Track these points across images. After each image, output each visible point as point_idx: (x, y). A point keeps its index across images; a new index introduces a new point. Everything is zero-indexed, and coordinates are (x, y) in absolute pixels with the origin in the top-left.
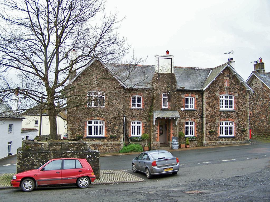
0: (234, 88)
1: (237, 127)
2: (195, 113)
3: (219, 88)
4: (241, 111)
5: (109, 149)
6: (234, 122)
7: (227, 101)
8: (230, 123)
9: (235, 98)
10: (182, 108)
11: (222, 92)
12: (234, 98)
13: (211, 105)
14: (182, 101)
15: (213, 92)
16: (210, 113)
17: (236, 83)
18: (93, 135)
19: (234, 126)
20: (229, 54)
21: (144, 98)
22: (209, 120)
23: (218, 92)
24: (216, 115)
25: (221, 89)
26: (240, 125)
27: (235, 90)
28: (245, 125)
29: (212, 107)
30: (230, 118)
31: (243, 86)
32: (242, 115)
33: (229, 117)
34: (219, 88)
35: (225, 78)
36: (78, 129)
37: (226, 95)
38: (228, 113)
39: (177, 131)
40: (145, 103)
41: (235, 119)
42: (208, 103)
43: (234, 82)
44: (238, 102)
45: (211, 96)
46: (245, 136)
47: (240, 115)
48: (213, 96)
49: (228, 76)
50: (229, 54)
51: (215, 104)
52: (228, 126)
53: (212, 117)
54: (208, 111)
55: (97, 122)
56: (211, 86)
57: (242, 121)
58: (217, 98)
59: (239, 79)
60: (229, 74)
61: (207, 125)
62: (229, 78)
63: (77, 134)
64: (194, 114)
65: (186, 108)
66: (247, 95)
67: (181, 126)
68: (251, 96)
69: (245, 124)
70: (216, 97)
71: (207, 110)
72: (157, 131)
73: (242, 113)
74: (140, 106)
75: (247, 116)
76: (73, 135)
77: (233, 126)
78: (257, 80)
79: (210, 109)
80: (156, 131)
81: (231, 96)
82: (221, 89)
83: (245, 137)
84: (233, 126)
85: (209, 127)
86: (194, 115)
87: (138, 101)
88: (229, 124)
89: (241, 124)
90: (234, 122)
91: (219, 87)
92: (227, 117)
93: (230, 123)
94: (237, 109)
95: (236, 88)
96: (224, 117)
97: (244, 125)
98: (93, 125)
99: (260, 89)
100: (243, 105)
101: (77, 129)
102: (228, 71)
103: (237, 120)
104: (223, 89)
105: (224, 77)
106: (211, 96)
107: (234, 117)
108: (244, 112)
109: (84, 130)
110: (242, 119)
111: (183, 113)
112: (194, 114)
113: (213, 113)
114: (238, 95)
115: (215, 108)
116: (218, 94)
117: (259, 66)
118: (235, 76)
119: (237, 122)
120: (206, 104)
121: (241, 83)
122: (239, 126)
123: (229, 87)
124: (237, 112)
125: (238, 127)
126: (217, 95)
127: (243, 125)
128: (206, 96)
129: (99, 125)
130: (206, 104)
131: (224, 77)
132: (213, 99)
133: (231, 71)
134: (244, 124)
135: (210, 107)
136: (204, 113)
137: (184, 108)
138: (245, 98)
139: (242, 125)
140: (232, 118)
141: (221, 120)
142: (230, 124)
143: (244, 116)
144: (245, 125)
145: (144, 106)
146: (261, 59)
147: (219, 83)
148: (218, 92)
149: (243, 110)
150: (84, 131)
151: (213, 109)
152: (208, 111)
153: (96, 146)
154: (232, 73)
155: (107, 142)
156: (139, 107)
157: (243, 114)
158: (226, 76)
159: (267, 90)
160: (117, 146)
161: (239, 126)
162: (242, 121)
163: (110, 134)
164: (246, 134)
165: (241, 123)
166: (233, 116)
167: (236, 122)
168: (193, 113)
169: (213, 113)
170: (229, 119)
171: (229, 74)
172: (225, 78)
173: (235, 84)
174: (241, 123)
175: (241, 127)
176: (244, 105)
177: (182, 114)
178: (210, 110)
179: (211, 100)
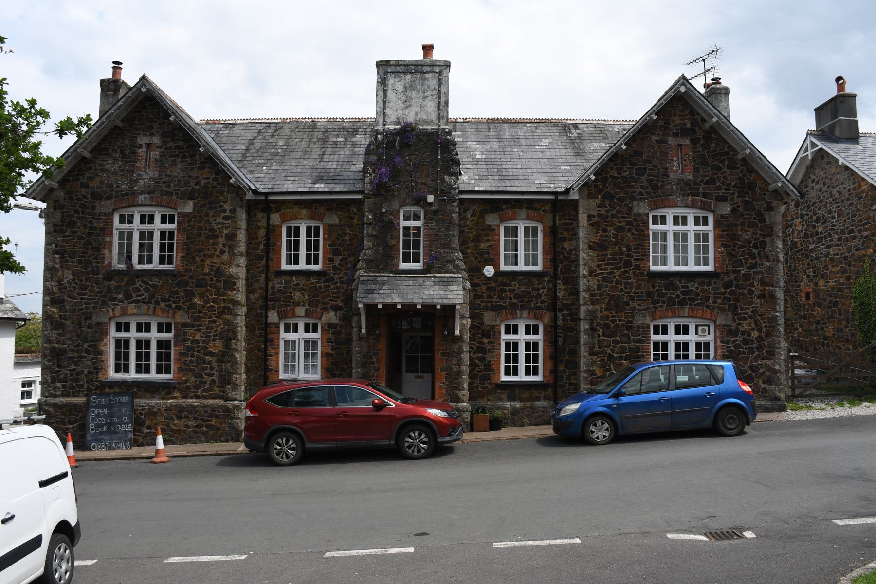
0: (711, 181)
1: (728, 342)
2: (543, 288)
3: (647, 181)
4: (747, 277)
5: (187, 426)
6: (715, 322)
7: (682, 241)
8: (700, 328)
9: (717, 224)
10: (487, 267)
11: (661, 199)
12: (715, 221)
13: (610, 251)
14: (485, 238)
15: (621, 200)
16: (607, 286)
17: (723, 161)
18: (133, 375)
19: (716, 340)
20: (704, 60)
21: (329, 228)
22: (604, 313)
23: (641, 199)
24: (635, 293)
25: (655, 187)
26: (743, 333)
27: (719, 188)
28: (763, 335)
29: (616, 259)
30: (699, 304)
31: (751, 170)
32: (751, 292)
33: (694, 300)
34: (647, 181)
35: (671, 141)
36: (77, 351)
37: (680, 212)
38: (689, 285)
39: (462, 359)
40: (334, 250)
41: (722, 310)
42: (597, 246)
43: (713, 156)
44: (734, 237)
45: (613, 216)
46: (764, 383)
47: (742, 294)
48: (620, 216)
49: (684, 132)
50: (704, 60)
51: (629, 249)
52: (692, 338)
53: (615, 304)
54: (600, 278)
55: (150, 323)
56: (611, 177)
57: (750, 317)
58: (638, 225)
59: (734, 146)
60: (689, 126)
61: (593, 337)
62: (688, 142)
63: (74, 370)
64: (540, 292)
65: (503, 268)
66: (770, 208)
67: (485, 340)
68: (808, 226)
69: (764, 330)
70: (635, 220)
71: (591, 273)
72: (378, 360)
73: (752, 285)
74: (316, 263)
75: (773, 297)
76: (58, 372)
77: (710, 338)
78: (829, 163)
79: (605, 269)
80: (371, 358)
81: (701, 213)
82: (655, 187)
83: (768, 387)
84: (710, 338)
85: (605, 343)
86: (539, 296)
87: (308, 243)
88: (692, 329)
89: (747, 328)
90: (715, 322)
91: (644, 178)
92: (682, 303)
93: (697, 326)
94: (730, 268)
95: (723, 183)
96: (671, 303)
97: (759, 337)
98: (133, 335)
99: (840, 193)
100: (754, 250)
101: (72, 351)
102: (688, 121)
103: (730, 314)
104: (662, 186)
105: (670, 138)
106: (613, 216)
107: (714, 302)
108: (762, 282)
109: (98, 355)
110: (753, 312)
111: (493, 289)
112: (540, 292)
113: (623, 287)
114: (733, 211)
115: (628, 264)
116: (641, 208)
117: (836, 116)
118: (716, 132)
119: (729, 322)
120: (590, 248)
121: (744, 160)
122: (740, 338)
123: (690, 177)
124: (726, 279)
125: (733, 342)
126: (635, 210)
127: (755, 334)
128: (589, 216)
129: (154, 335)
130: (590, 248)
131: (670, 138)
132: (619, 229)
133: (698, 114)
134: (760, 330)
135: (609, 259)
136: (583, 284)
137: (496, 266)
138: (764, 221)
139: (749, 334)
140: (707, 307)
141: (658, 315)
142: (700, 333)
143: (762, 296)
144: (763, 335)
145: (331, 260)
146: (841, 82)
147: (645, 161)
148: (644, 199)
149: (756, 273)
150: (97, 359)
151: (620, 268)
152: (600, 278)
153: (141, 414)
154: (704, 121)
155: (182, 402)
156: (312, 267)
157: (757, 289)
158: (676, 135)
159: (867, 195)
160: (217, 417)
161: (740, 338)
162: (750, 317)
163: (191, 370)
164: (768, 373)
165: (746, 326)
166: (712, 296)
167: (724, 322)
168: (534, 289)
169: (623, 287)
170: (691, 309)
171: (689, 126)
172: (671, 141)
173: (717, 163)
174: (746, 326)
175: (746, 342)
176: (759, 253)
177: (488, 293)
178: (608, 273)
179: (611, 231)
